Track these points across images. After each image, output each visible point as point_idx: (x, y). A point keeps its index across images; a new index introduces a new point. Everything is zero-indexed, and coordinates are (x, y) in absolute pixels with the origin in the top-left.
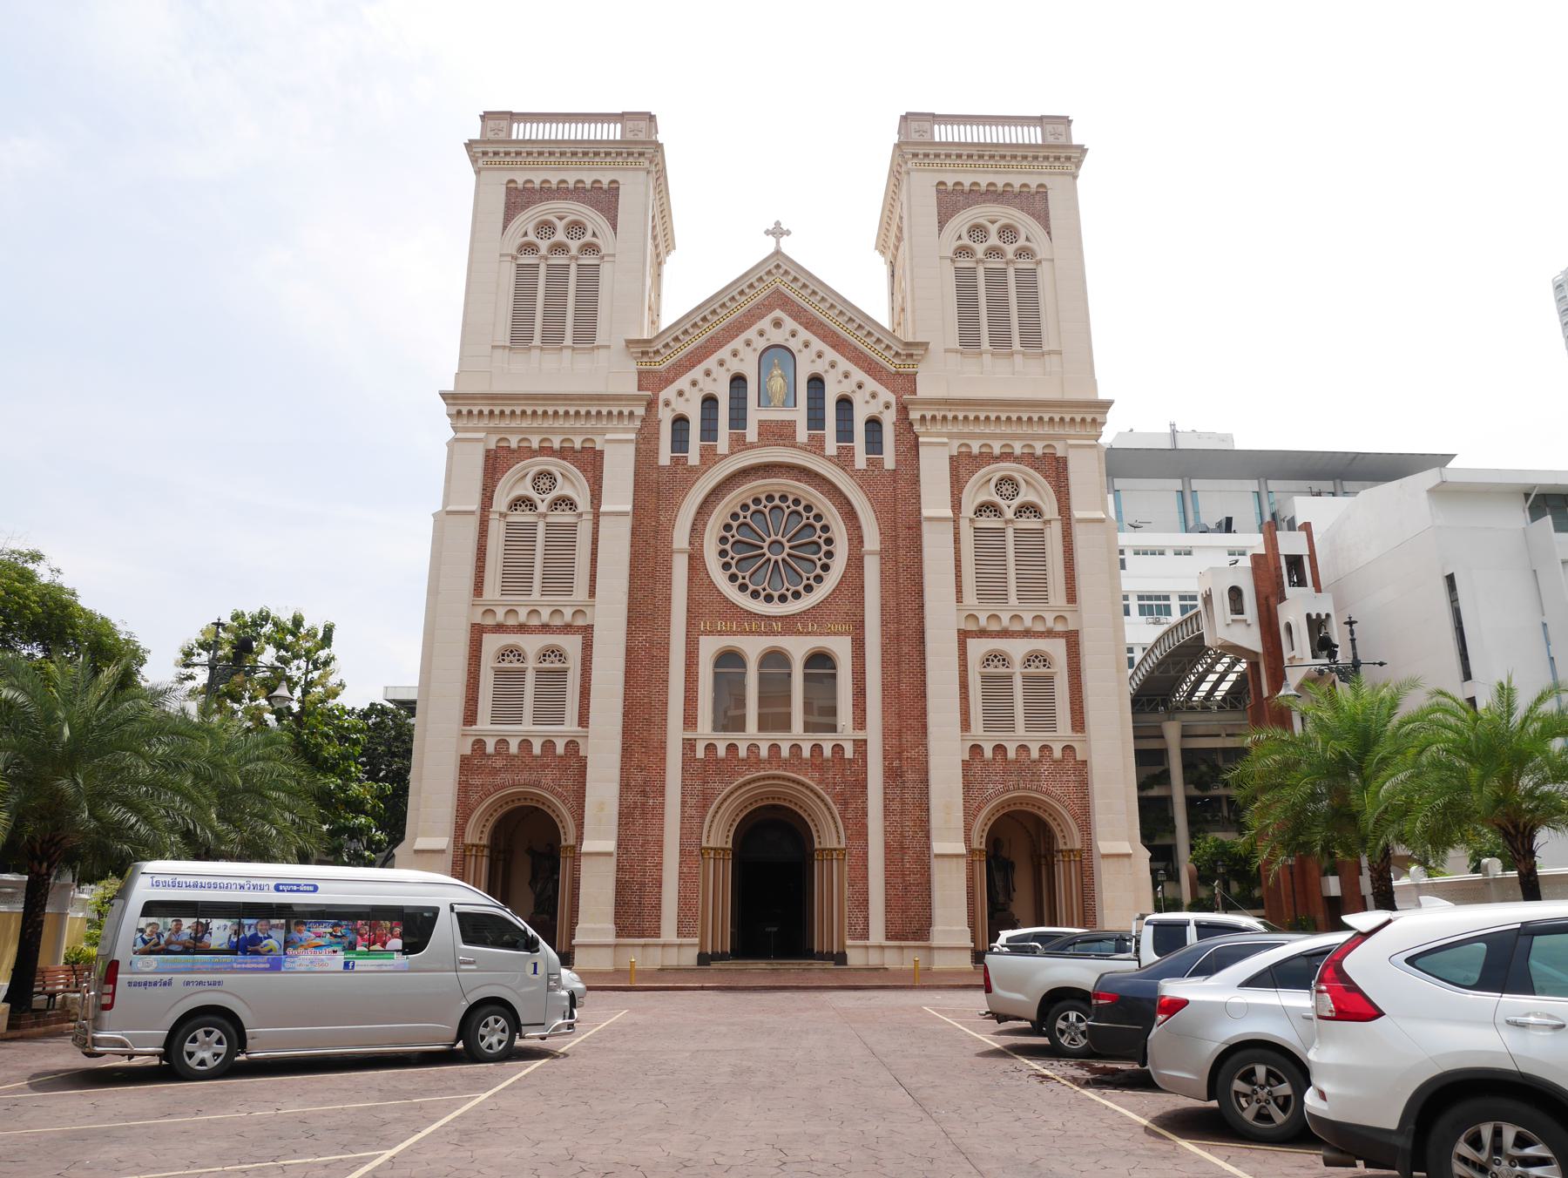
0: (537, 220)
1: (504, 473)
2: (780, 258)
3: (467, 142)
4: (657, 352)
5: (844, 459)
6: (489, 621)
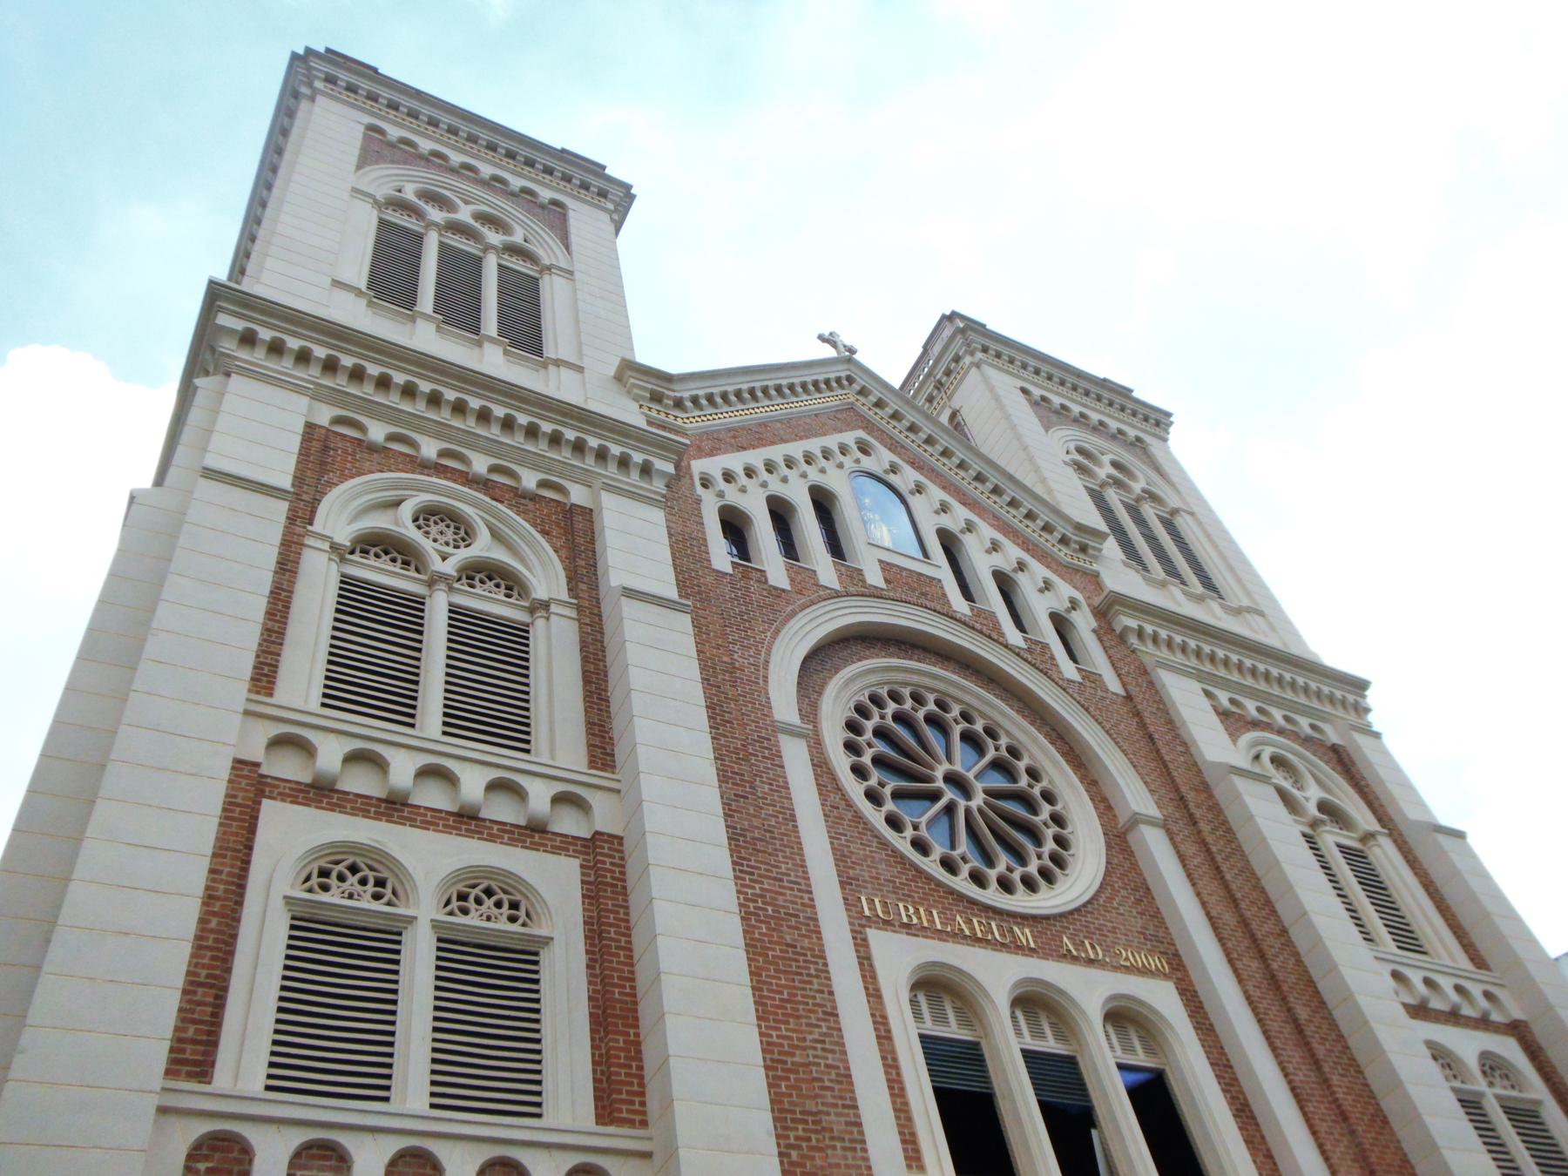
0: (421, 185)
1: (344, 477)
2: (852, 367)
3: (301, 51)
4: (679, 404)
5: (1036, 656)
6: (288, 768)
